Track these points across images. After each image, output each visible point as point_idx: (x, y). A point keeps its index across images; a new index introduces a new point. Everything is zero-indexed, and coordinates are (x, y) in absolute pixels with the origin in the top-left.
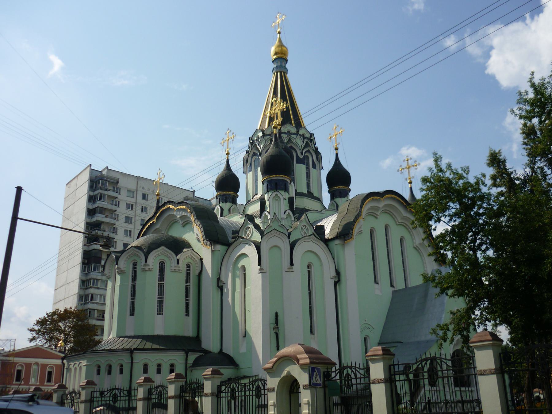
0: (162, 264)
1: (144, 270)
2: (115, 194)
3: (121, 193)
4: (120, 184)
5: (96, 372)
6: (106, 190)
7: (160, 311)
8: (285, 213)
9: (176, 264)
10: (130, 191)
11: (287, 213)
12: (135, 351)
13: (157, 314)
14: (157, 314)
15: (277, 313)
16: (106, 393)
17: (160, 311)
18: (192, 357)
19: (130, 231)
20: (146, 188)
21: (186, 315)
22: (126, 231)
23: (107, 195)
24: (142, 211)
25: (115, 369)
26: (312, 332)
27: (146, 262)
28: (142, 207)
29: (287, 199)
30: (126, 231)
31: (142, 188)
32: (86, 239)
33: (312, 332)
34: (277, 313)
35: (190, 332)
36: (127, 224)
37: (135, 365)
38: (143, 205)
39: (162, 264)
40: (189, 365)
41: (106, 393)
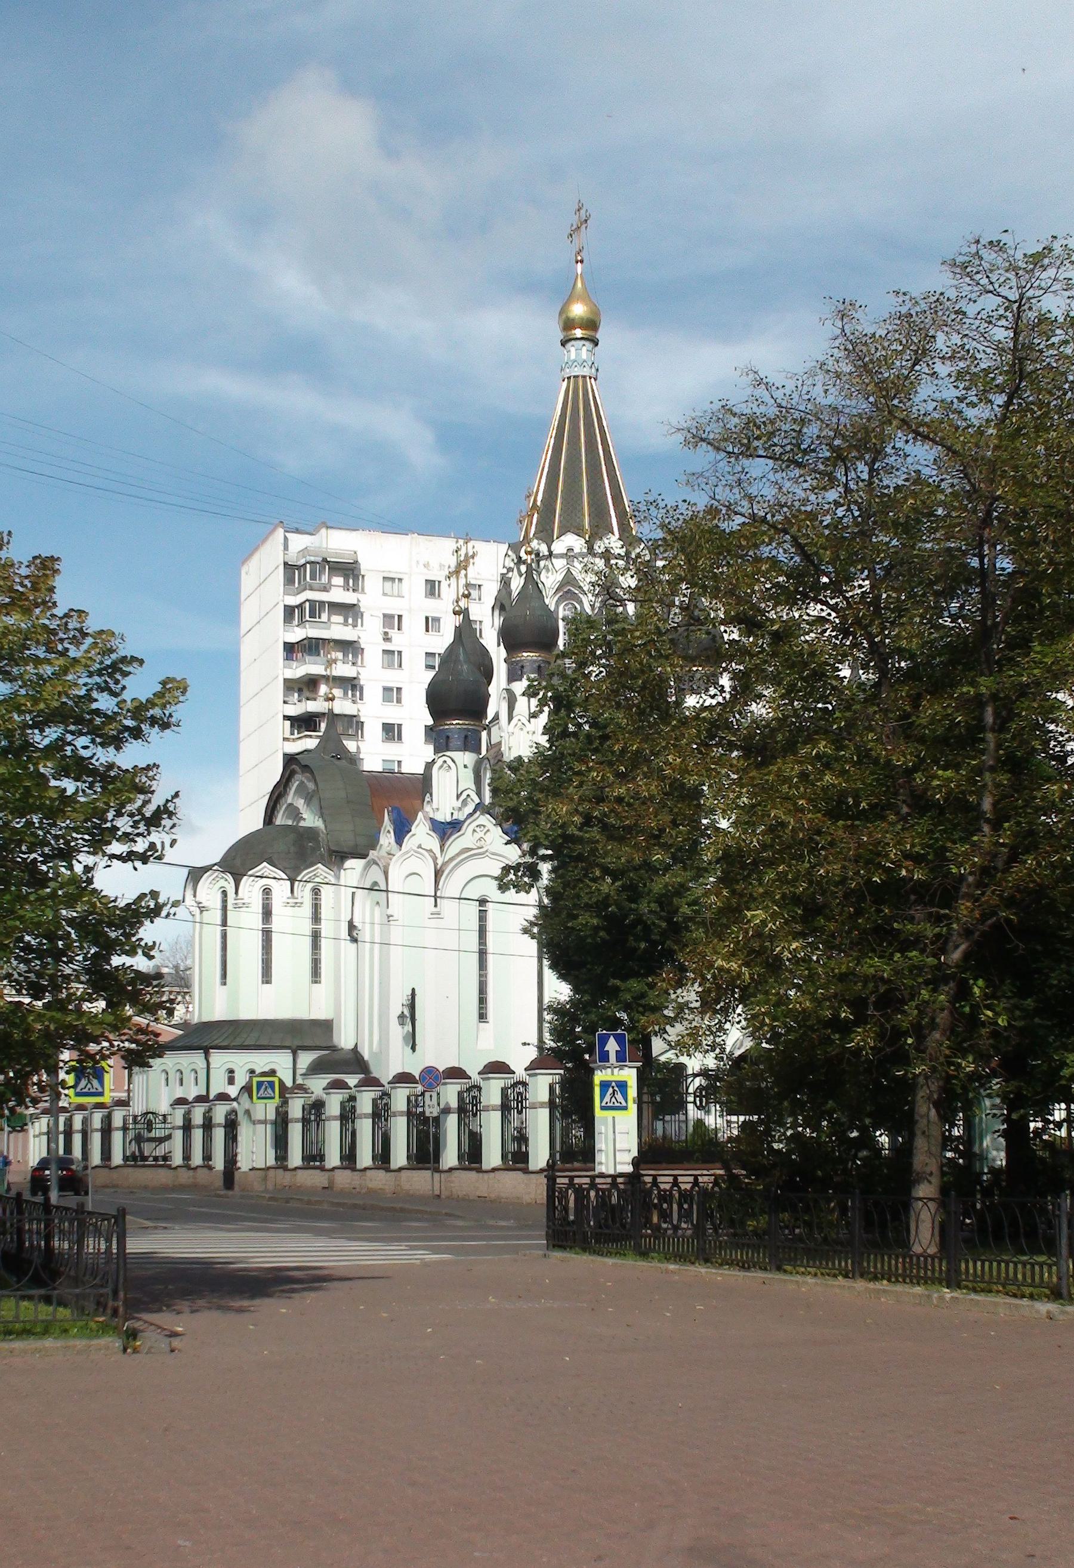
0: (267, 892)
1: (237, 907)
2: (349, 598)
3: (366, 590)
4: (364, 567)
5: (163, 1082)
6: (325, 589)
7: (267, 976)
8: (458, 797)
9: (290, 895)
10: (393, 579)
11: (464, 796)
12: (211, 1051)
13: (263, 983)
14: (263, 983)
15: (413, 990)
16: (139, 1118)
17: (267, 976)
18: (306, 1059)
19: (399, 689)
20: (434, 564)
21: (316, 982)
22: (387, 690)
23: (328, 602)
24: (427, 630)
25: (189, 1078)
26: (482, 1016)
27: (236, 893)
28: (427, 618)
29: (471, 766)
30: (387, 690)
31: (424, 566)
32: (288, 723)
33: (482, 1016)
34: (413, 990)
35: (320, 1012)
36: (389, 672)
37: (212, 1071)
38: (430, 614)
39: (267, 892)
40: (299, 1072)
41: (139, 1118)
